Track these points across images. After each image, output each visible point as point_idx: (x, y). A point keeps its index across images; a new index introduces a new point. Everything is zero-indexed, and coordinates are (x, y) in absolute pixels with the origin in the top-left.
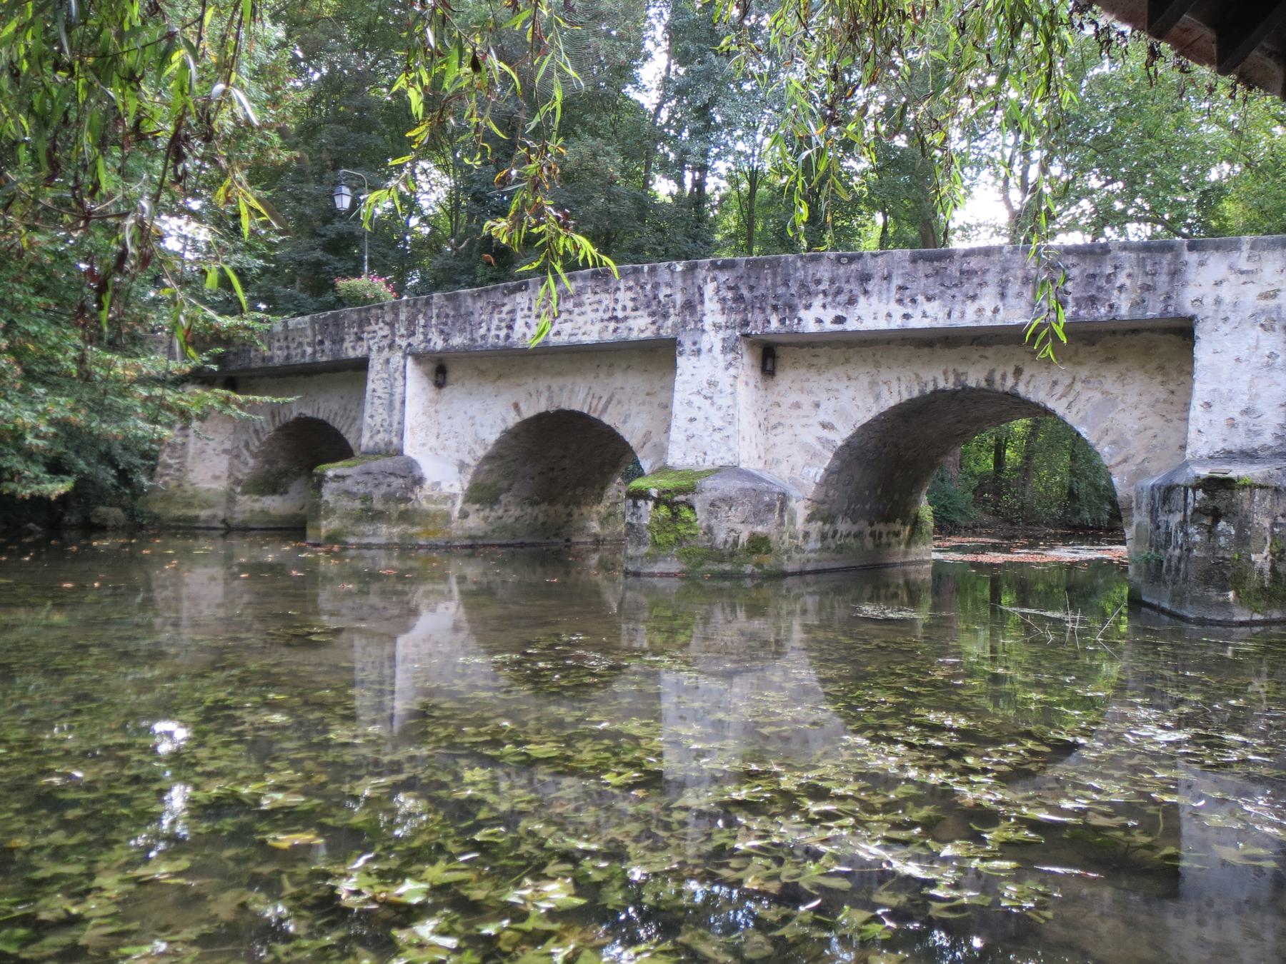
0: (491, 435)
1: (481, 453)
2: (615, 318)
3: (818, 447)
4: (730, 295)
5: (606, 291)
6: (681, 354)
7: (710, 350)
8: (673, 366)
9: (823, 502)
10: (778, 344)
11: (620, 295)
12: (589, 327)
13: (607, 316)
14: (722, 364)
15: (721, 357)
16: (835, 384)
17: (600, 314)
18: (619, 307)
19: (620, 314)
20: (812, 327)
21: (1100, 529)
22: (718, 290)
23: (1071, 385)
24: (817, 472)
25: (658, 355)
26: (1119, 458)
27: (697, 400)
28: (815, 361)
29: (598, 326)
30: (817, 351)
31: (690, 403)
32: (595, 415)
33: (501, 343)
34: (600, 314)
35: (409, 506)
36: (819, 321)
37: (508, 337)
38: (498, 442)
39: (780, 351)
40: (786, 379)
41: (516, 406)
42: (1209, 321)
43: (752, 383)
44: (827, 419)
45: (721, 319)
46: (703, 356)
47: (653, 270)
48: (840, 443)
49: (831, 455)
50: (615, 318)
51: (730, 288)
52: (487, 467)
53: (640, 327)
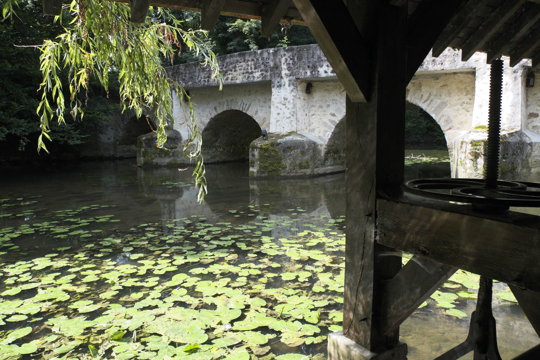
0: (207, 121)
1: (203, 127)
2: (247, 72)
3: (329, 123)
4: (291, 62)
5: (244, 61)
6: (273, 87)
7: (284, 85)
8: (271, 92)
9: (333, 146)
10: (313, 81)
11: (250, 63)
12: (238, 77)
13: (245, 71)
14: (289, 91)
15: (288, 88)
16: (336, 98)
17: (242, 71)
18: (249, 68)
19: (250, 71)
20: (323, 75)
21: (126, 277)
22: (286, 60)
23: (429, 97)
24: (329, 134)
25: (264, 88)
26: (448, 128)
27: (281, 106)
28: (327, 88)
29: (241, 77)
30: (329, 84)
31: (277, 107)
32: (244, 112)
33: (206, 84)
34: (242, 71)
35: (176, 150)
36: (326, 72)
37: (208, 81)
38: (209, 123)
39: (314, 84)
40: (317, 96)
41: (215, 108)
42: (482, 70)
43: (302, 98)
44: (333, 112)
45: (287, 72)
46: (282, 88)
47: (275, 54)
48: (338, 122)
49: (334, 127)
50: (247, 72)
51: (291, 59)
52: (206, 133)
53: (257, 76)
